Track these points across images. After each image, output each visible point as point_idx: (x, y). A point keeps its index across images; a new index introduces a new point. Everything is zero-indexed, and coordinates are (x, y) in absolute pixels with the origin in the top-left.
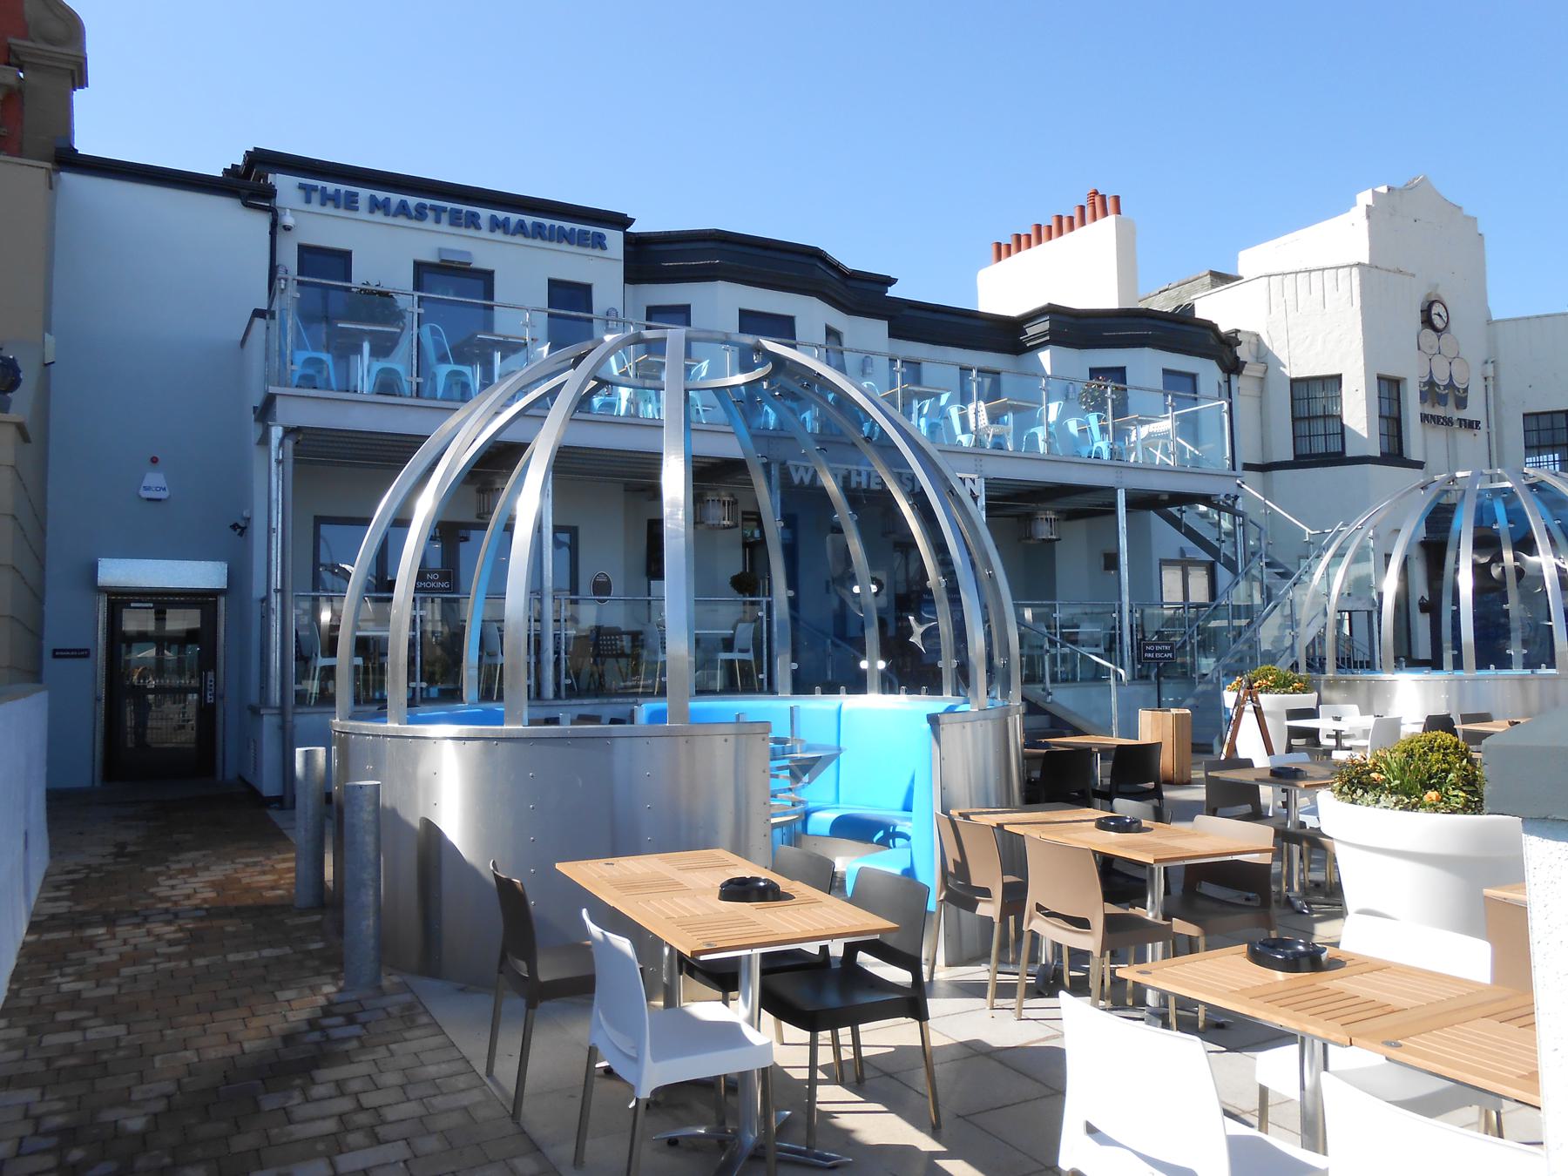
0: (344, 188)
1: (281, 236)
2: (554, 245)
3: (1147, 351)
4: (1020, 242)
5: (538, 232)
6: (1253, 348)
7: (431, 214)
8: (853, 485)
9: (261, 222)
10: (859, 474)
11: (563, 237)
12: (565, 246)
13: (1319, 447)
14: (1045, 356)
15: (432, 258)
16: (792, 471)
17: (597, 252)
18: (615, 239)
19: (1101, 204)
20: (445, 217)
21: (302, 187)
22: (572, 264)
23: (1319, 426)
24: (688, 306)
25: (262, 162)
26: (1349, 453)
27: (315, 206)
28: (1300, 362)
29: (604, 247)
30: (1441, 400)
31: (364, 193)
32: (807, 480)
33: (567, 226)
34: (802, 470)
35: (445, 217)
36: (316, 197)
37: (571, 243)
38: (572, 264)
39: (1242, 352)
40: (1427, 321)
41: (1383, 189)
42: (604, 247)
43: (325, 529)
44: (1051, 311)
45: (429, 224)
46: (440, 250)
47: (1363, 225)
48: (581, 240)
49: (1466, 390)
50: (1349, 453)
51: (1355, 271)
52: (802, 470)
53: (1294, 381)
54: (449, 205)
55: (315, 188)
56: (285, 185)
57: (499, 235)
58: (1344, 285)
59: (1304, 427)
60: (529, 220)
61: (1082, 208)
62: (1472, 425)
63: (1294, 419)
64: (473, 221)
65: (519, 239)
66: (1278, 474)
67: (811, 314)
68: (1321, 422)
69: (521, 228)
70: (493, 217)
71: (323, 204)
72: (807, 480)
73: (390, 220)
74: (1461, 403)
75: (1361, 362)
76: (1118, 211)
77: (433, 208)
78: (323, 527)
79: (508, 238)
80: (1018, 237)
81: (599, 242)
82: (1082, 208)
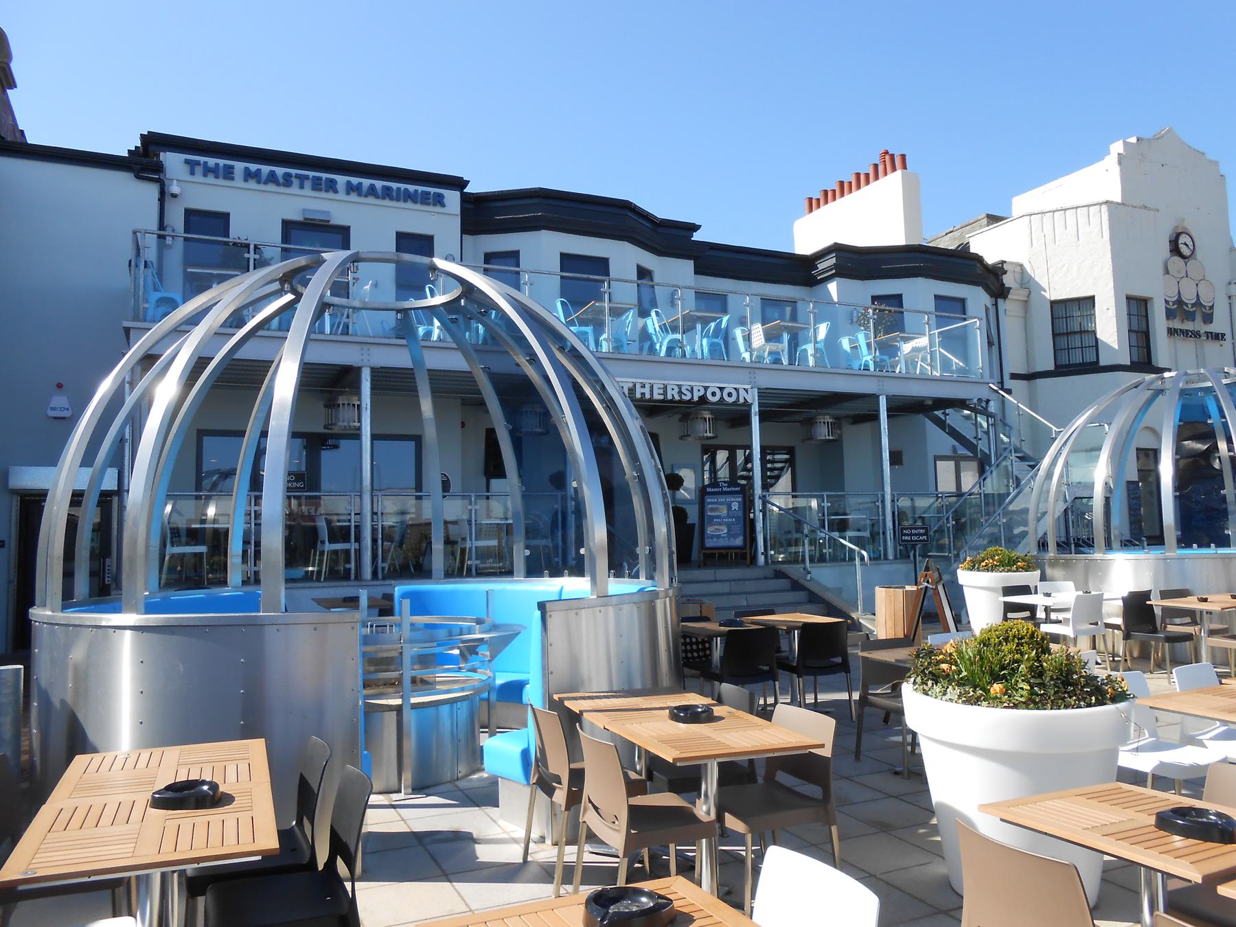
0: (222, 162)
1: (169, 203)
2: (401, 204)
3: (920, 280)
4: (828, 196)
5: (387, 194)
6: (1018, 276)
7: (296, 182)
8: (638, 396)
9: (152, 191)
10: (643, 386)
11: (408, 197)
12: (410, 205)
13: (1077, 358)
14: (832, 287)
15: (298, 217)
17: (438, 209)
18: (453, 198)
19: (891, 161)
20: (308, 184)
21: (187, 162)
22: (416, 219)
23: (1076, 341)
24: (518, 252)
25: (154, 143)
26: (1102, 363)
27: (199, 177)
28: (1059, 287)
29: (443, 205)
30: (1190, 316)
31: (239, 166)
33: (412, 188)
35: (308, 184)
36: (199, 170)
37: (415, 202)
38: (416, 219)
39: (1008, 280)
40: (1175, 249)
41: (1133, 140)
42: (443, 205)
43: (207, 440)
44: (837, 249)
45: (295, 189)
46: (304, 211)
47: (1115, 170)
48: (425, 199)
49: (1212, 307)
50: (1102, 363)
51: (1104, 208)
53: (1054, 304)
54: (311, 174)
55: (198, 163)
56: (173, 161)
57: (353, 197)
58: (1095, 220)
59: (1063, 341)
60: (379, 184)
61: (876, 166)
62: (1218, 337)
63: (1055, 335)
64: (331, 186)
65: (371, 200)
66: (1040, 382)
67: (624, 257)
68: (1078, 337)
69: (372, 191)
70: (349, 183)
71: (205, 175)
73: (262, 187)
74: (1208, 318)
75: (1111, 285)
76: (904, 167)
77: (297, 176)
78: (206, 439)
79: (362, 200)
80: (826, 192)
81: (439, 201)
82: (876, 166)
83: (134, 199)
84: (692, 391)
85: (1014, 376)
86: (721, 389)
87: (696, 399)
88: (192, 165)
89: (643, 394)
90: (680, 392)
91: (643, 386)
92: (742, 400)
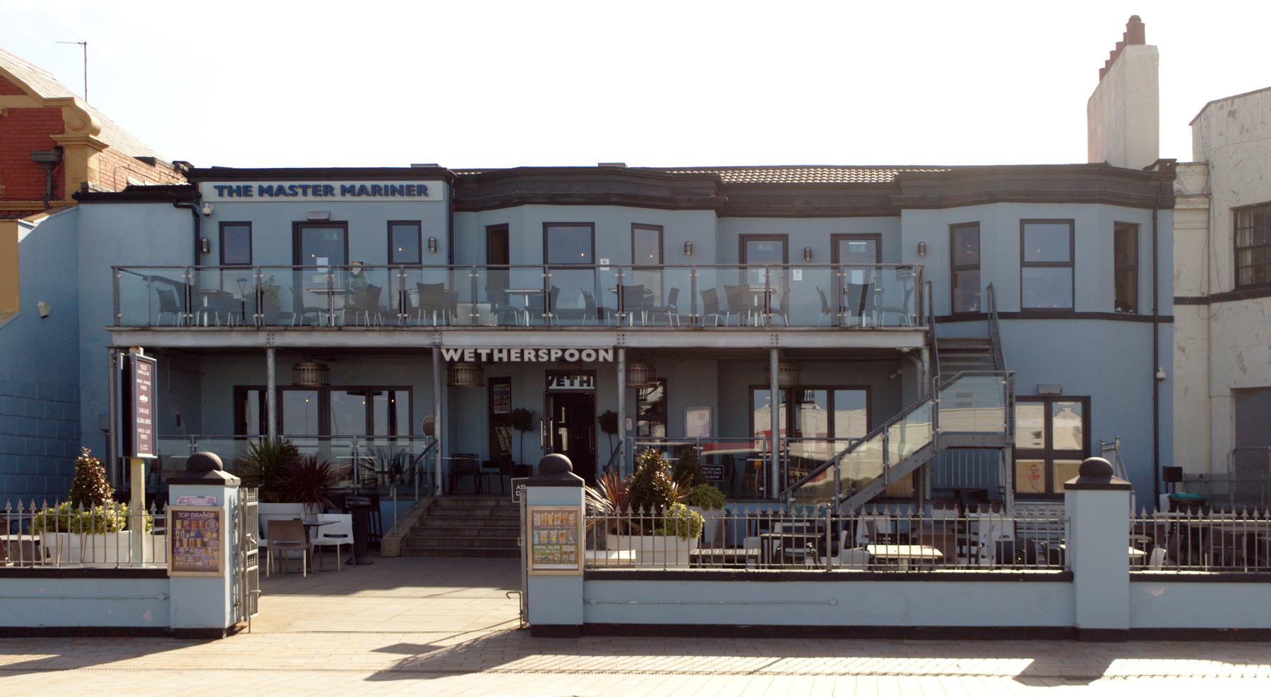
0: (242, 184)
1: (203, 221)
2: (390, 198)
5: (376, 190)
7: (300, 191)
8: (496, 359)
10: (500, 351)
11: (394, 191)
12: (398, 198)
16: (444, 352)
17: (423, 198)
20: (310, 191)
22: (401, 207)
24: (506, 225)
27: (226, 198)
29: (426, 195)
32: (456, 358)
33: (397, 184)
34: (452, 352)
35: (310, 191)
38: (401, 207)
42: (426, 195)
45: (300, 198)
48: (409, 191)
52: (452, 352)
56: (207, 188)
60: (368, 184)
64: (329, 191)
70: (343, 187)
72: (456, 358)
73: (274, 199)
77: (300, 186)
81: (423, 191)
83: (176, 220)
84: (549, 354)
85: (1180, 301)
86: (580, 351)
87: (553, 359)
88: (220, 190)
89: (501, 359)
90: (537, 356)
91: (500, 351)
92: (601, 359)
